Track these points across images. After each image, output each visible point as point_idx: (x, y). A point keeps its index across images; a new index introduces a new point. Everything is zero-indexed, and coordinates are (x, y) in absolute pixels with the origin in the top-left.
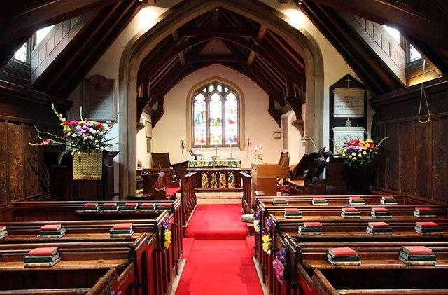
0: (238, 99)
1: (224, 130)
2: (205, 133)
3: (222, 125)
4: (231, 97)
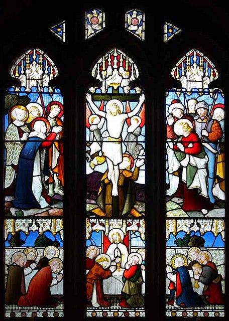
2: (54, 253)
3: (146, 217)
4: (195, 74)
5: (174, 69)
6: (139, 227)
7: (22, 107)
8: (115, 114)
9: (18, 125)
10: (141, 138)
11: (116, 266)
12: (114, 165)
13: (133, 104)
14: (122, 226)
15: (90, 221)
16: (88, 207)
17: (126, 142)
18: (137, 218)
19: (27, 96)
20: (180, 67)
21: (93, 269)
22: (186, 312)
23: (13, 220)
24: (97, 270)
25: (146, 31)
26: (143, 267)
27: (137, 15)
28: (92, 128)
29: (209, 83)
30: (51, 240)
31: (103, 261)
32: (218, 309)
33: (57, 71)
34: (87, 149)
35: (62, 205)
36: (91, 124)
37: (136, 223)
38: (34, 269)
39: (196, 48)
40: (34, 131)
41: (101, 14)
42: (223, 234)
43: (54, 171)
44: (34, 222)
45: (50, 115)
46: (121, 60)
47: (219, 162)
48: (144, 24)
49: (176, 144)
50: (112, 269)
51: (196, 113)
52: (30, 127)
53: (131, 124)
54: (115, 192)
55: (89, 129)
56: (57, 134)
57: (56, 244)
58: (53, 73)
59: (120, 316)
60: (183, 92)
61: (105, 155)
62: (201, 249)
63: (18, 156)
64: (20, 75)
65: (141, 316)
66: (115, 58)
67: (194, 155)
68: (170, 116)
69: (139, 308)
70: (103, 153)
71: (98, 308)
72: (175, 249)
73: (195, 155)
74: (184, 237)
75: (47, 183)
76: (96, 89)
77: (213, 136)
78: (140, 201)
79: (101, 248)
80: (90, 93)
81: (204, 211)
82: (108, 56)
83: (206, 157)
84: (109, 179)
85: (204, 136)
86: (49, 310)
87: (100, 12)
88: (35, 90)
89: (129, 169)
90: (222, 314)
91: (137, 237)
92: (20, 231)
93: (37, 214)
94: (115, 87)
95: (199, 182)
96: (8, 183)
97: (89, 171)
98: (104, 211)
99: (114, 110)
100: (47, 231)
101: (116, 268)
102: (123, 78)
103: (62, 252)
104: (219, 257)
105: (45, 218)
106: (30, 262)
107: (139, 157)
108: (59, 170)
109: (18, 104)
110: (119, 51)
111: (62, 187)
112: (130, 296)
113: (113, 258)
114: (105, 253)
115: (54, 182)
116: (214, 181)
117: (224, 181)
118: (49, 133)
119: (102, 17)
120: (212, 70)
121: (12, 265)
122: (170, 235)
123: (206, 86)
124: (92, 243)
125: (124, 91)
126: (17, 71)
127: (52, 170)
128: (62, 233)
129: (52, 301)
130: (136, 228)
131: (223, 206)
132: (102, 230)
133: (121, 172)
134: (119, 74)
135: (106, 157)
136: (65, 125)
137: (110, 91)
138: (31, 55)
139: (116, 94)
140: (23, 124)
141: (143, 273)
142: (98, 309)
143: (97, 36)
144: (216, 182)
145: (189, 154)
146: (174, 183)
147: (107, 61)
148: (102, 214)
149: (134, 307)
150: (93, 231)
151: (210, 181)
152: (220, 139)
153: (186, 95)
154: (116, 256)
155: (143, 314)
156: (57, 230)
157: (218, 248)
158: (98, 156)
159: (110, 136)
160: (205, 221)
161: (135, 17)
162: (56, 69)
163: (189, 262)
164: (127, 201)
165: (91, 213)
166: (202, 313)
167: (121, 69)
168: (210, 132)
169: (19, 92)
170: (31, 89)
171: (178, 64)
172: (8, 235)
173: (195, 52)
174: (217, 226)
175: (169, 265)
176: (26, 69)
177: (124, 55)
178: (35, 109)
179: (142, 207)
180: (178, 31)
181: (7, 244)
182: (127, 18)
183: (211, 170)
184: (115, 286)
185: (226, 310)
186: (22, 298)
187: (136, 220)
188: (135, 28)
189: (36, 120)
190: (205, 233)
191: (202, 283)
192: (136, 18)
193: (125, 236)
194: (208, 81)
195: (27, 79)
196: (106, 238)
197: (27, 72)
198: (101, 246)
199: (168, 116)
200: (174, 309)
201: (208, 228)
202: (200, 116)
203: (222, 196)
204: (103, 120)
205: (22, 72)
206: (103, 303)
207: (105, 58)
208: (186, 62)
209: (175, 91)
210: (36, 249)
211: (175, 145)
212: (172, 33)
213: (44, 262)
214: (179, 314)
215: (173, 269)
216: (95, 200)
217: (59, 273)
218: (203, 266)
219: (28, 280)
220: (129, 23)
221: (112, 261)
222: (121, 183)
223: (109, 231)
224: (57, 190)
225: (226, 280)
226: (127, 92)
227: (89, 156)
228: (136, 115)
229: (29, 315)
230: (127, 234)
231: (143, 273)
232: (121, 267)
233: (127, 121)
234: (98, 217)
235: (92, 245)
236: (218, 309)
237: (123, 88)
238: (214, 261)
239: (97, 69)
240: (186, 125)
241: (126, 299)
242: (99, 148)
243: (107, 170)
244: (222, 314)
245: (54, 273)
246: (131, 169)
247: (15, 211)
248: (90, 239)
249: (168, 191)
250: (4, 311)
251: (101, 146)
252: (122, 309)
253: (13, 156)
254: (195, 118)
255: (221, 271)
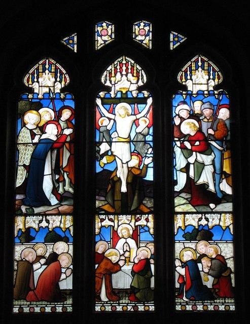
0: (231, 88)
1: (164, 238)
4: (200, 80)
5: (180, 74)
6: (148, 222)
7: (35, 112)
8: (123, 116)
9: (30, 128)
10: (149, 138)
11: (125, 260)
12: (123, 163)
13: (141, 106)
14: (131, 221)
15: (99, 217)
16: (98, 204)
17: (134, 142)
18: (145, 214)
19: (39, 102)
20: (186, 72)
21: (103, 264)
22: (195, 305)
23: (23, 217)
24: (106, 264)
25: (154, 40)
26: (152, 261)
27: (144, 26)
28: (101, 129)
29: (213, 85)
30: (60, 236)
31: (112, 255)
32: (228, 303)
33: (68, 79)
34: (97, 148)
35: (72, 202)
36: (100, 125)
37: (145, 218)
38: (44, 265)
39: (199, 54)
40: (46, 133)
41: (110, 27)
42: (231, 227)
43: (64, 170)
44: (44, 219)
45: (61, 119)
46: (130, 67)
47: (226, 159)
48: (151, 34)
49: (183, 143)
50: (121, 263)
51: (201, 114)
52: (42, 129)
53: (139, 125)
54: (124, 189)
55: (99, 130)
56: (67, 136)
57: (66, 240)
58: (65, 80)
59: (129, 310)
60: (189, 94)
61: (114, 154)
62: (209, 243)
63: (30, 157)
64: (33, 83)
65: (150, 310)
66: (124, 65)
67: (200, 152)
68: (177, 116)
69: (148, 301)
70: (112, 153)
71: (107, 302)
72: (184, 243)
73: (201, 152)
74: (193, 230)
75: (58, 181)
76: (105, 94)
77: (219, 134)
78: (149, 197)
79: (110, 243)
80: (100, 97)
81: (212, 206)
82: (117, 64)
83: (213, 154)
84: (118, 177)
85: (210, 134)
86: (57, 304)
87: (110, 25)
88: (47, 96)
89: (137, 167)
90: (232, 308)
91: (146, 231)
92: (29, 228)
93: (47, 211)
94: (124, 92)
95: (206, 178)
96: (19, 182)
97: (99, 170)
98: (113, 207)
99: (123, 112)
100: (56, 227)
101: (125, 262)
102: (131, 83)
103: (71, 247)
104: (227, 250)
105: (55, 215)
106: (39, 258)
107: (147, 155)
108: (69, 168)
109: (31, 109)
110: (128, 59)
111: (71, 185)
112: (139, 290)
113: (122, 252)
114: (114, 247)
115: (64, 180)
116: (221, 177)
117: (231, 177)
118: (60, 135)
119: (111, 29)
120: (216, 73)
121: (22, 260)
122: (178, 229)
123: (211, 88)
124: (101, 238)
125: (132, 95)
126: (30, 79)
127: (63, 169)
128: (72, 229)
129: (60, 296)
130: (145, 223)
131: (231, 200)
132: (111, 226)
133: (130, 170)
134: (127, 80)
135: (115, 156)
136: (76, 128)
137: (119, 96)
138: (44, 64)
139: (125, 98)
140: (35, 127)
141: (152, 267)
142: (107, 303)
143: (107, 47)
144: (223, 177)
145: (196, 152)
146: (181, 180)
147: (116, 68)
148: (111, 210)
149: (143, 301)
150: (102, 226)
151: (217, 177)
152: (226, 137)
153: (192, 97)
154: (125, 250)
155: (152, 308)
156: (67, 226)
157: (227, 241)
158: (108, 155)
159: (118, 137)
160: (213, 215)
161: (143, 27)
162: (67, 76)
163: (198, 255)
164: (136, 198)
165: (100, 209)
166: (212, 307)
167: (130, 75)
168: (216, 131)
169: (33, 99)
170: (43, 95)
171: (183, 69)
172: (18, 232)
173: (200, 58)
174: (225, 220)
175: (177, 259)
176: (39, 78)
177: (133, 62)
178: (47, 113)
179: (150, 202)
180: (183, 39)
181: (17, 240)
182: (135, 29)
183: (218, 166)
184: (123, 280)
185: (236, 304)
186: (31, 293)
187: (144, 216)
188: (143, 38)
189: (47, 123)
190: (213, 227)
191: (213, 276)
192: (143, 29)
193: (133, 231)
194: (212, 83)
195: (39, 86)
196: (115, 233)
197: (40, 80)
198: (110, 241)
199: (175, 117)
200: (184, 303)
201: (216, 222)
202: (206, 116)
203: (228, 190)
204: (112, 121)
205: (36, 80)
206: (112, 297)
207: (114, 65)
208: (192, 67)
209: (182, 94)
210: (45, 245)
211: (182, 144)
212: (178, 41)
213: (54, 257)
214: (189, 308)
215: (182, 262)
216: (105, 197)
217: (68, 268)
218: (212, 259)
219: (37, 274)
220: (137, 33)
221: (120, 256)
222: (130, 181)
223: (118, 226)
224: (67, 188)
225: (236, 273)
226: (135, 95)
227: (99, 156)
228: (144, 116)
229: (37, 310)
230: (135, 229)
231: (152, 267)
232: (130, 261)
233: (136, 123)
234: (107, 213)
235: (101, 240)
236: (228, 303)
237: (131, 92)
238: (223, 254)
239: (106, 75)
240: (193, 125)
241: (135, 294)
242: (109, 148)
243: (116, 169)
244: (232, 308)
245: (63, 268)
246: (139, 166)
247: (26, 209)
248: (99, 234)
249: (176, 187)
250: (12, 306)
251: (110, 146)
252: (131, 303)
253: (25, 156)
254: (201, 118)
255: (231, 264)
